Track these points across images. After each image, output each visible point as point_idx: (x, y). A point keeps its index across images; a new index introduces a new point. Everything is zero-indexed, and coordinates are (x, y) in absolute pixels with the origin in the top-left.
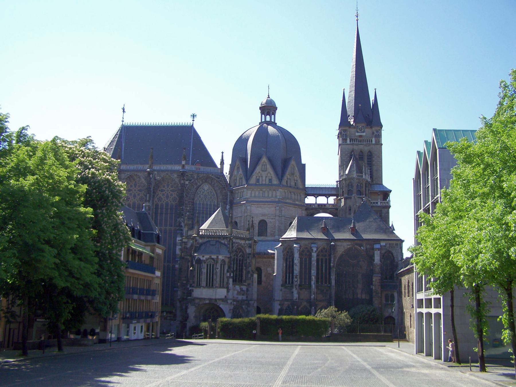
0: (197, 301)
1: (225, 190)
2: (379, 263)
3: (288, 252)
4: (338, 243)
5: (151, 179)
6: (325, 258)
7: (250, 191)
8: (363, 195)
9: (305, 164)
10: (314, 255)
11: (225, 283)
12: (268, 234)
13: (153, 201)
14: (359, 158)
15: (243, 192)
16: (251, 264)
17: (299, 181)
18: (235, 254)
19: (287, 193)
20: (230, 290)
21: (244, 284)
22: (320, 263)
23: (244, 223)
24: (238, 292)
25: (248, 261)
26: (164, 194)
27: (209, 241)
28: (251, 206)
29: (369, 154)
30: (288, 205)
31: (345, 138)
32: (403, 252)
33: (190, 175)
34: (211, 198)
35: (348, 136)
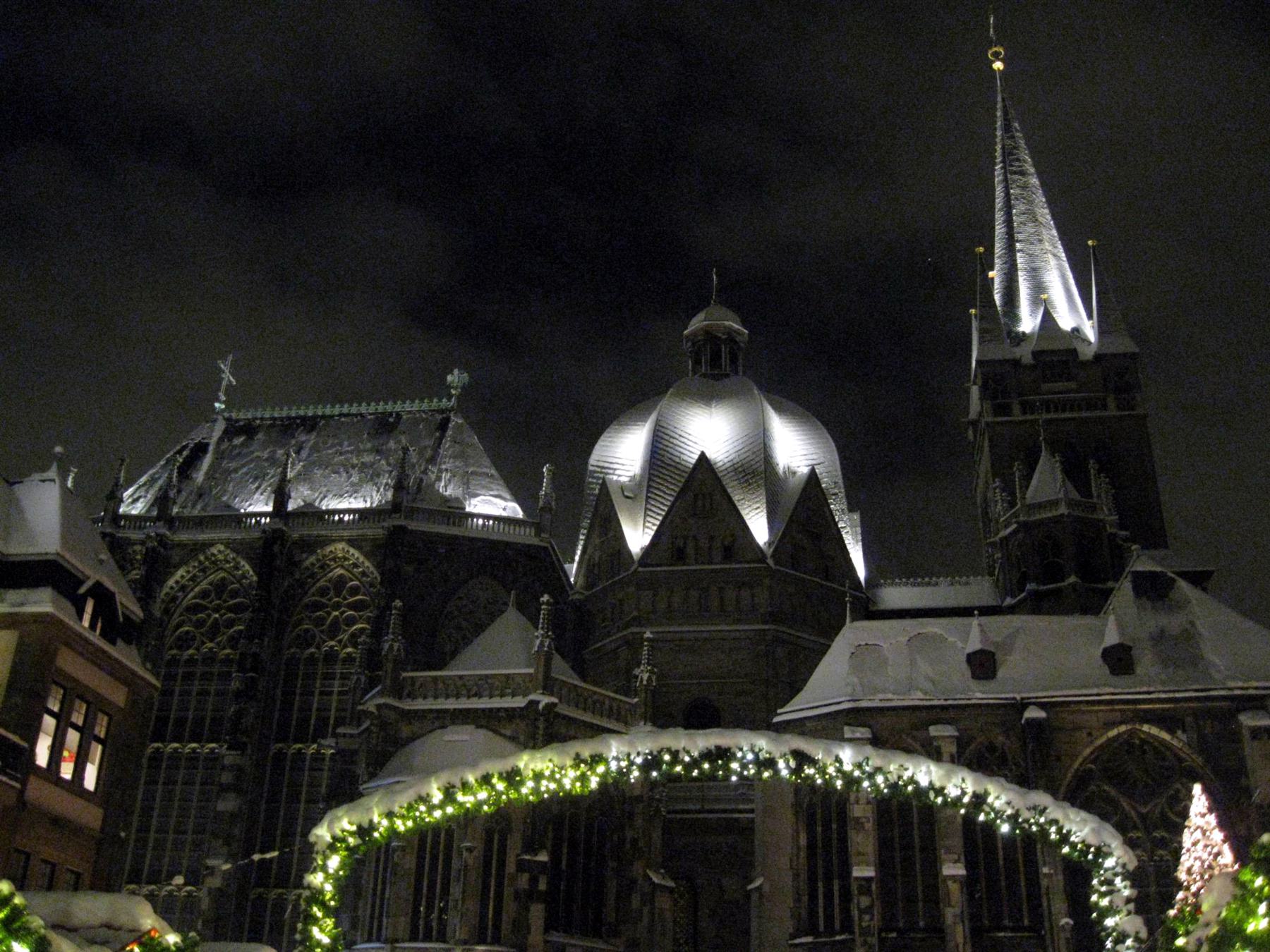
11: (506, 927)
16: (641, 844)
25: (629, 834)
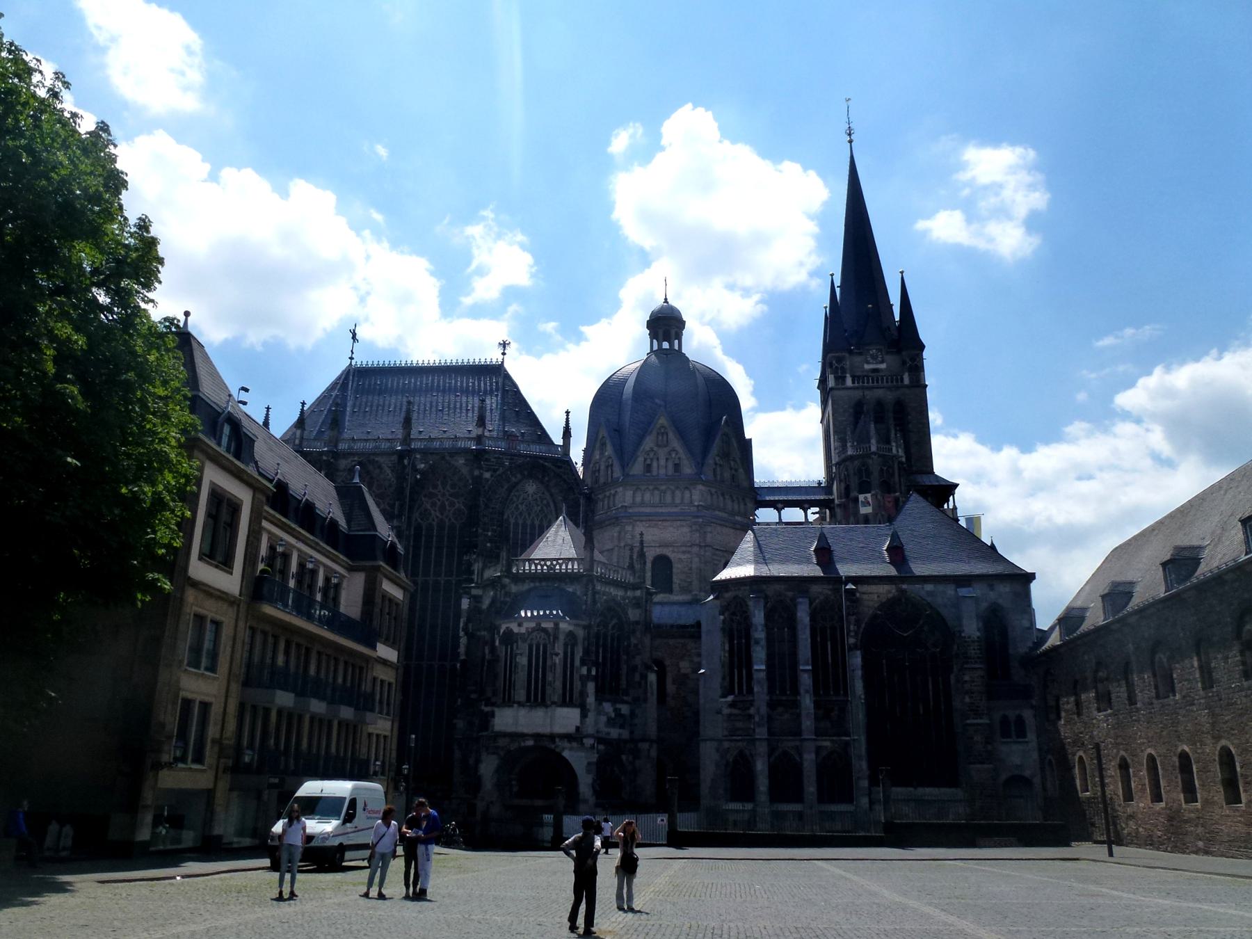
0: (502, 742)
1: (574, 494)
3: (734, 614)
5: (404, 467)
7: (632, 492)
8: (895, 492)
9: (751, 439)
10: (803, 615)
11: (576, 694)
12: (676, 587)
13: (409, 518)
15: (614, 495)
16: (640, 646)
17: (741, 470)
19: (715, 497)
20: (589, 710)
21: (625, 698)
24: (609, 719)
25: (634, 641)
26: (436, 503)
27: (535, 588)
28: (634, 526)
30: (719, 522)
31: (840, 374)
33: (495, 458)
34: (542, 510)
35: (848, 371)
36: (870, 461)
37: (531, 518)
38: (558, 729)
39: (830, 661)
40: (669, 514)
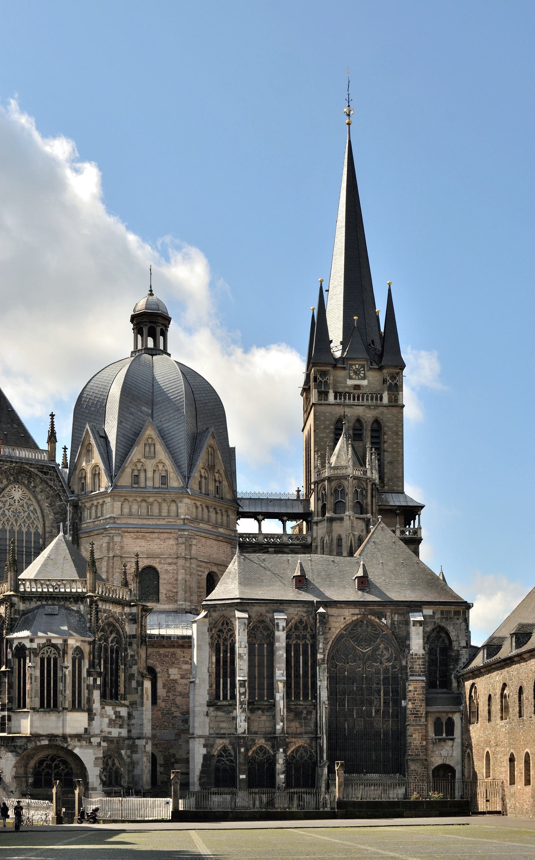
1: (61, 501)
2: (421, 652)
4: (333, 611)
6: (303, 642)
9: (234, 448)
10: (281, 635)
11: (84, 701)
14: (354, 434)
15: (102, 505)
16: (136, 658)
17: (225, 483)
18: (102, 635)
19: (200, 509)
20: (95, 715)
21: (123, 702)
22: (293, 654)
23: (107, 572)
24: (111, 720)
25: (130, 652)
29: (375, 426)
30: (203, 534)
31: (323, 389)
32: (470, 629)
34: (28, 517)
35: (331, 386)
36: (346, 483)
37: (18, 524)
38: (69, 731)
39: (301, 673)
40: (158, 526)
